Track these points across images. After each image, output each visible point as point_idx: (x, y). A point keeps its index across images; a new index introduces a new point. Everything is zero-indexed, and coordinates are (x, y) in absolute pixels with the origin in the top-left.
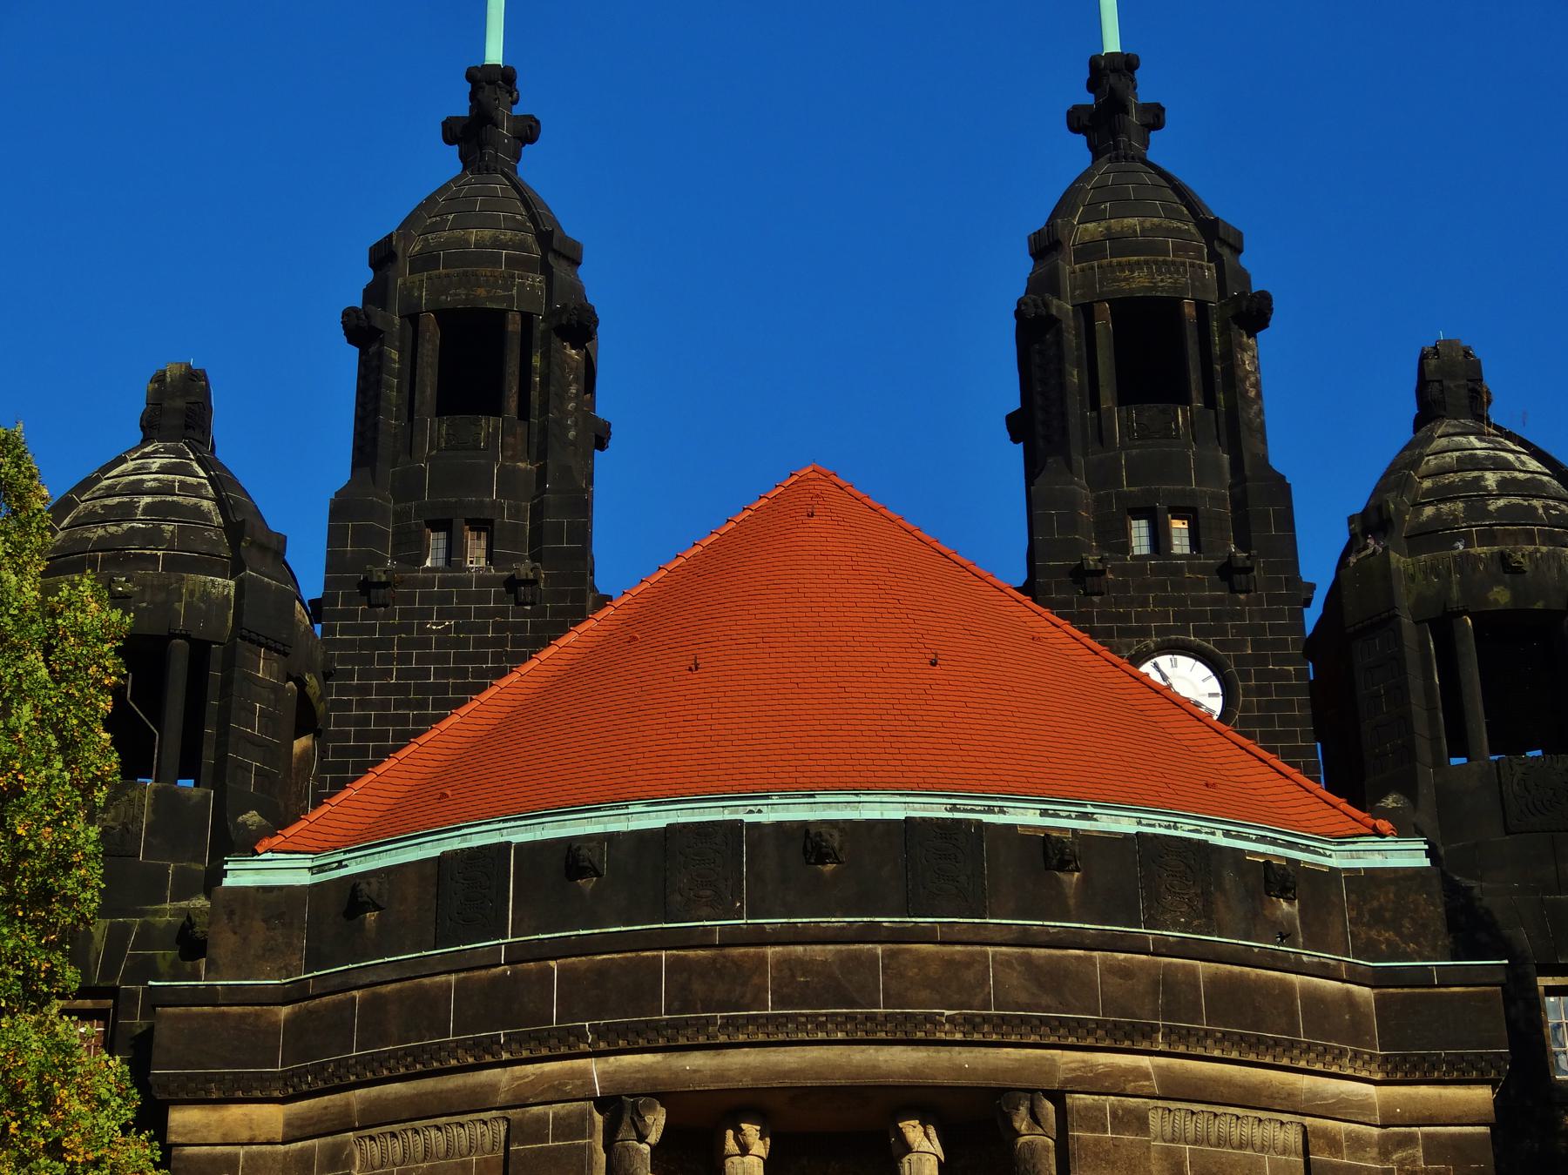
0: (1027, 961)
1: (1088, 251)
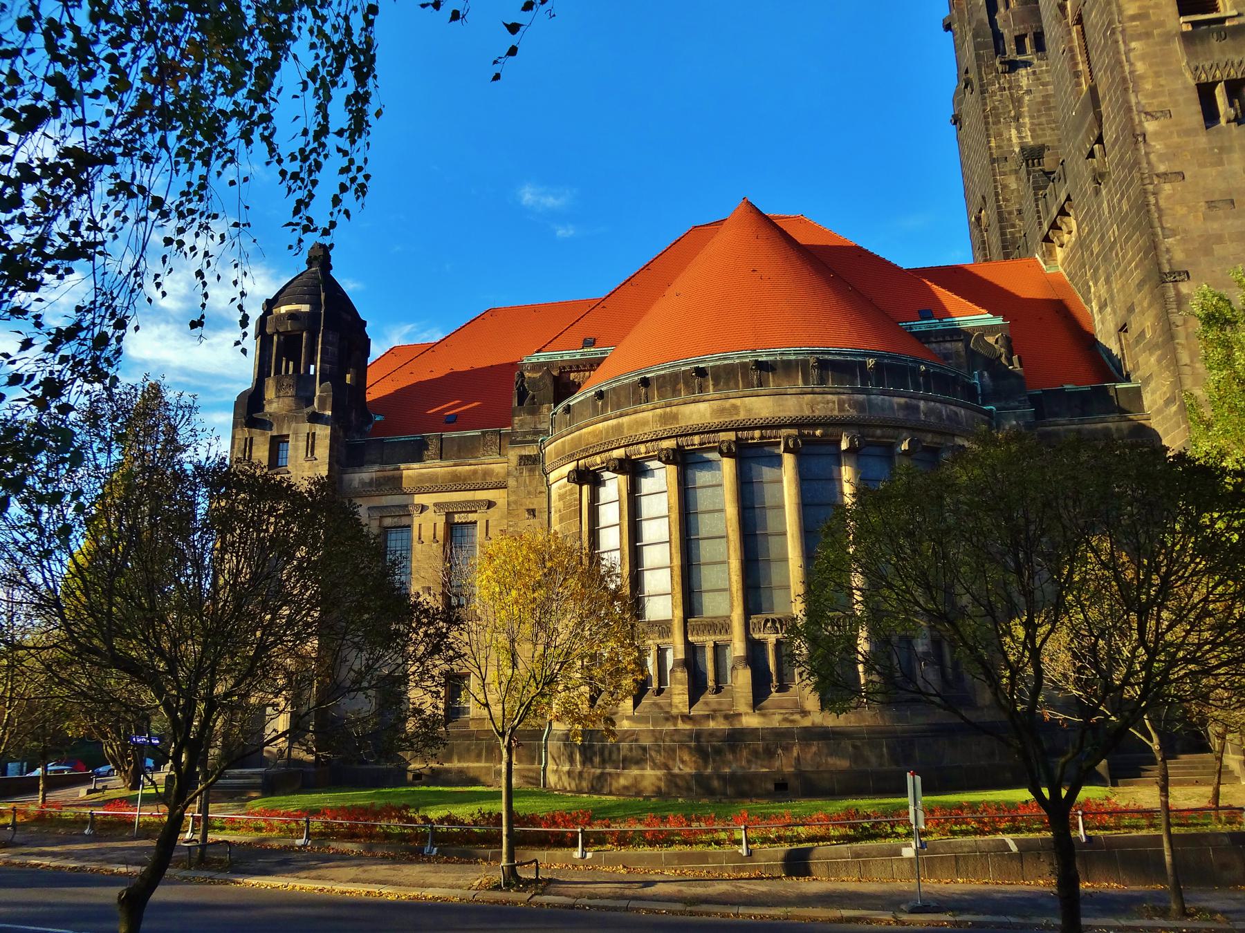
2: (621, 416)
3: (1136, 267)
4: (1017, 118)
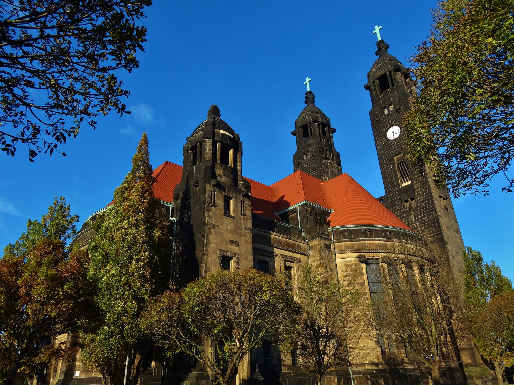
2: (386, 241)
3: (429, 237)
4: (328, 173)
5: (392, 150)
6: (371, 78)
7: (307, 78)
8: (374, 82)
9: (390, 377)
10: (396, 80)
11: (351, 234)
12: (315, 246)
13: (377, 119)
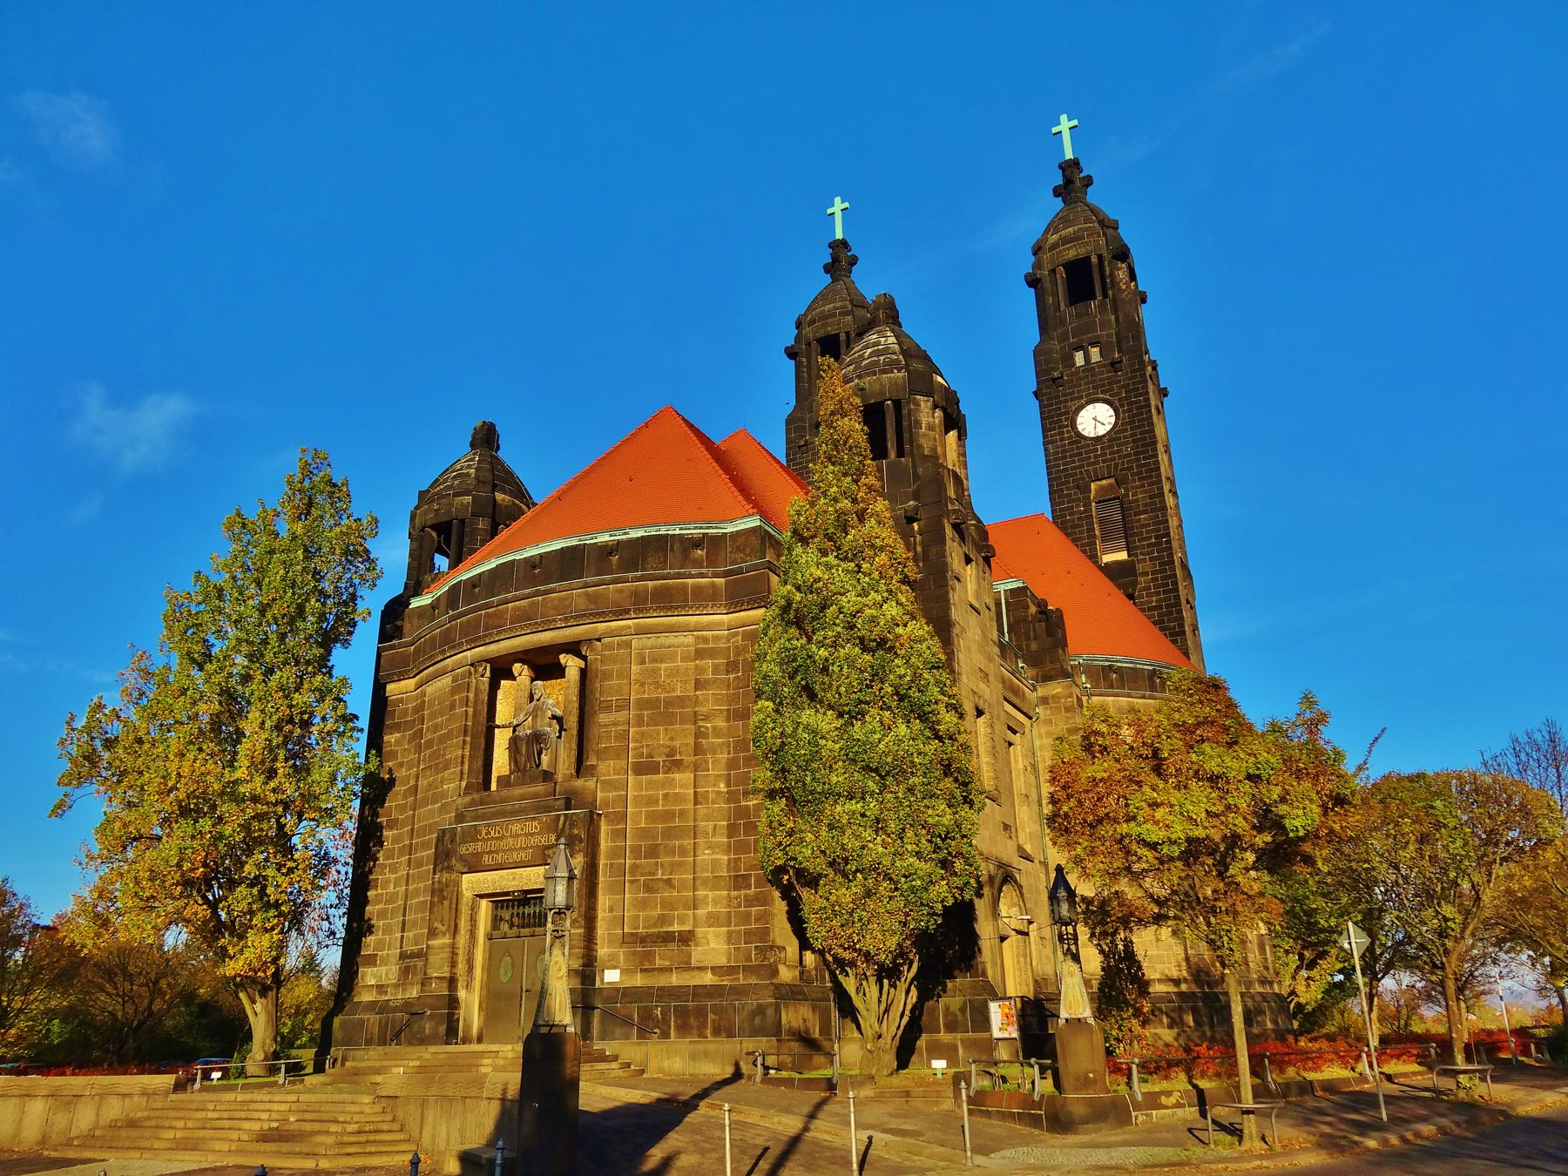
0: (587, 594)
1: (1055, 246)
5: (1090, 464)
6: (1046, 257)
7: (838, 200)
8: (1053, 271)
9: (1203, 1011)
10: (1114, 283)
11: (1122, 679)
12: (1056, 698)
13: (1056, 374)
